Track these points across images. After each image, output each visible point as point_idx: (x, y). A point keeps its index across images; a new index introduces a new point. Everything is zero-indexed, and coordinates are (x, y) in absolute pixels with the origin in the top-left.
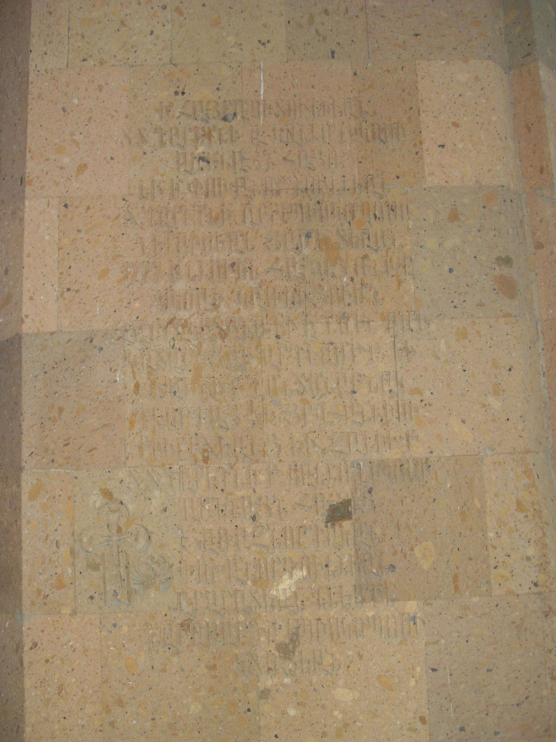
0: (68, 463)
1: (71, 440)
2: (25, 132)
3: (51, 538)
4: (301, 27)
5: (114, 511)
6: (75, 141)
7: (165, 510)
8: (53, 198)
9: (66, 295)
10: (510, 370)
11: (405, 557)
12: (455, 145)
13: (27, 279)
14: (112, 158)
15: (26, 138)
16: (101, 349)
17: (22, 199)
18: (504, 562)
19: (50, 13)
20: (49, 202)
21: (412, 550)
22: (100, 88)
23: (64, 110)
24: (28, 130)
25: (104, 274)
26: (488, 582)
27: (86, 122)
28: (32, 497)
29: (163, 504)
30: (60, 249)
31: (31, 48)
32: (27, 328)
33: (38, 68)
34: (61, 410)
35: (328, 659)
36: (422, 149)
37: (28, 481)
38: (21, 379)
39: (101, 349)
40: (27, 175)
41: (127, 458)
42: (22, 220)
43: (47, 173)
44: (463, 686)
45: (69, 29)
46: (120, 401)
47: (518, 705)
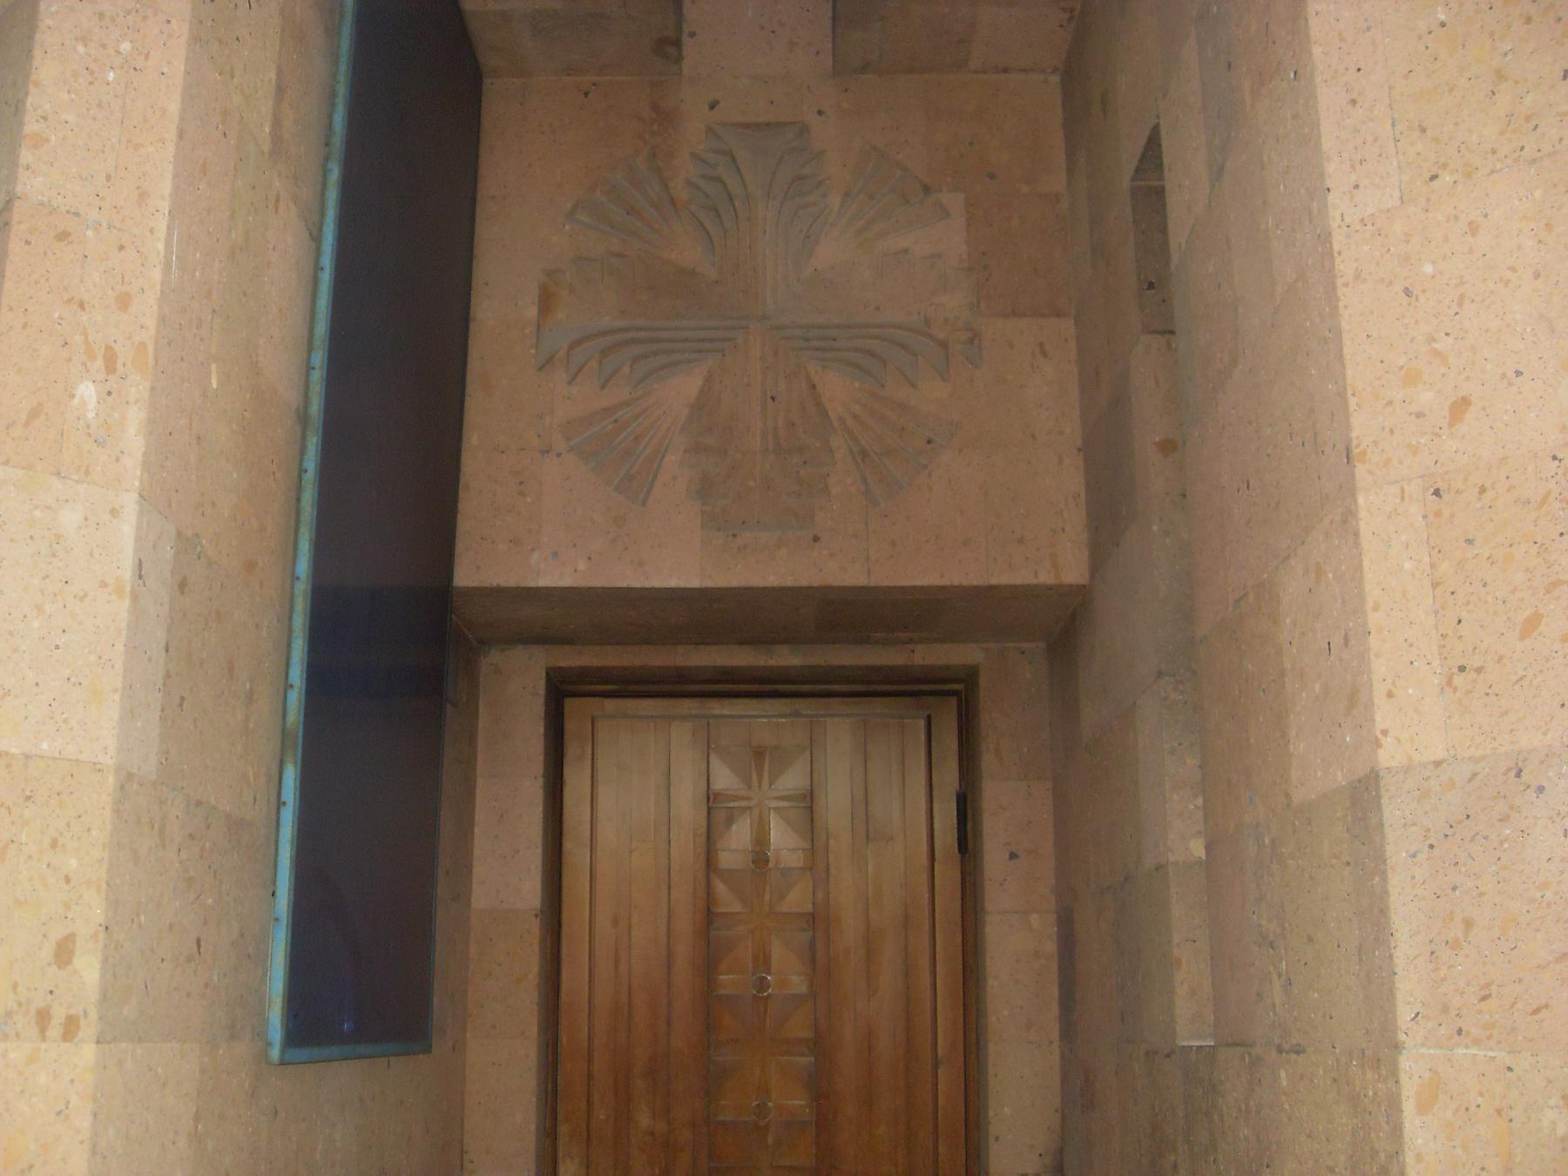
0: (1489, 1038)
1: (1494, 988)
2: (1341, 357)
6: (1437, 353)
8: (1410, 480)
9: (1458, 680)
13: (1377, 655)
14: (1518, 373)
15: (1344, 367)
16: (1541, 789)
17: (1353, 494)
19: (1354, 102)
20: (1403, 490)
22: (1473, 228)
23: (1407, 292)
24: (1345, 351)
27: (1455, 308)
28: (1423, 1107)
30: (1435, 585)
31: (1328, 183)
32: (1389, 756)
33: (1348, 220)
34: (1468, 924)
37: (1413, 1068)
38: (1385, 862)
40: (1355, 442)
42: (1356, 534)
43: (1392, 431)
45: (1393, 125)
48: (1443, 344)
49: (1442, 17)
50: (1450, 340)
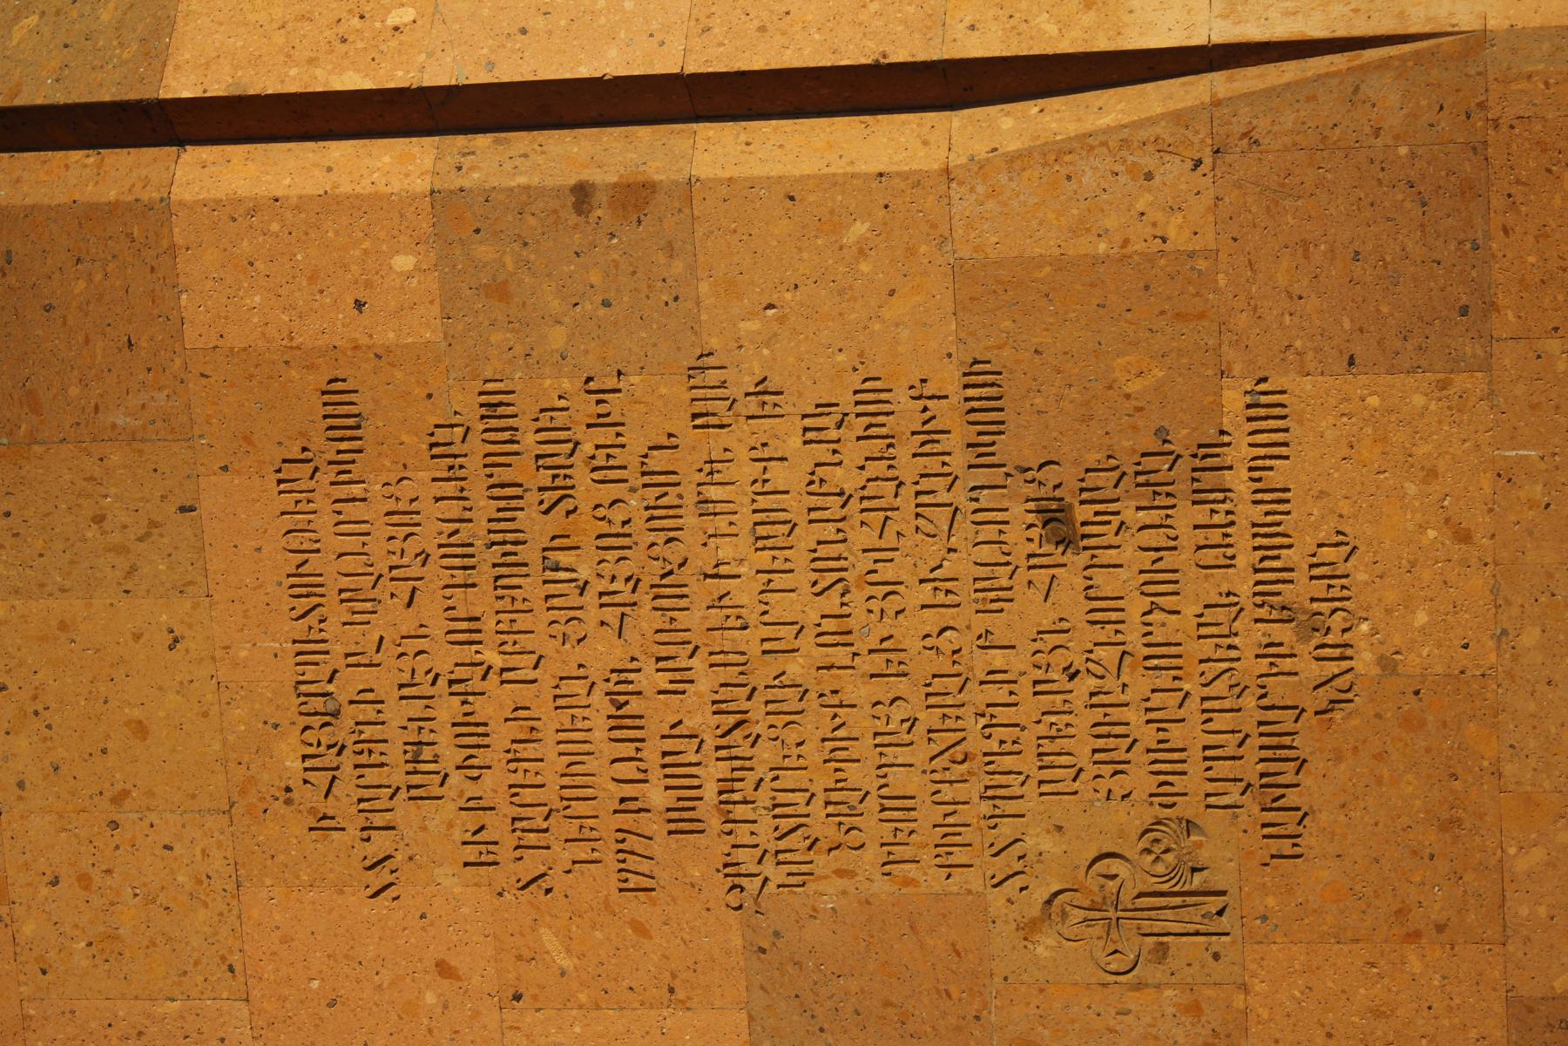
3: (1112, 1023)
4: (133, 570)
5: (1064, 914)
7: (1059, 828)
9: (680, 994)
10: (792, 198)
11: (1140, 409)
12: (356, 282)
14: (423, 916)
16: (777, 934)
18: (1154, 225)
20: (511, 1028)
21: (1128, 396)
25: (640, 929)
26: (1192, 255)
29: (1048, 832)
30: (598, 1007)
35: (1327, 554)
36: (369, 348)
39: (777, 934)
41: (969, 892)
44: (1385, 310)
46: (868, 902)
47: (1424, 204)
48: (386, 977)
49: (83, 944)
50: (383, 971)
